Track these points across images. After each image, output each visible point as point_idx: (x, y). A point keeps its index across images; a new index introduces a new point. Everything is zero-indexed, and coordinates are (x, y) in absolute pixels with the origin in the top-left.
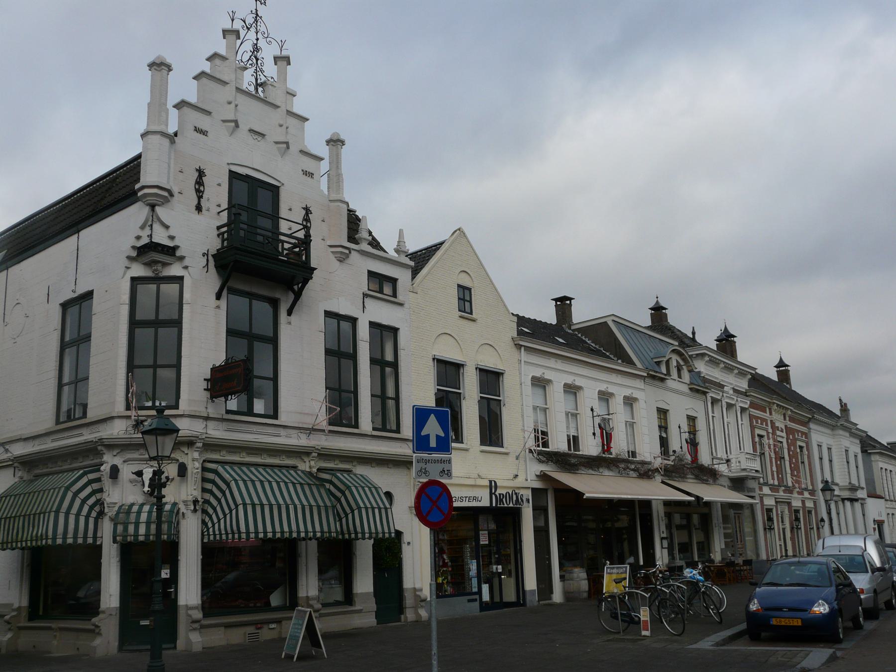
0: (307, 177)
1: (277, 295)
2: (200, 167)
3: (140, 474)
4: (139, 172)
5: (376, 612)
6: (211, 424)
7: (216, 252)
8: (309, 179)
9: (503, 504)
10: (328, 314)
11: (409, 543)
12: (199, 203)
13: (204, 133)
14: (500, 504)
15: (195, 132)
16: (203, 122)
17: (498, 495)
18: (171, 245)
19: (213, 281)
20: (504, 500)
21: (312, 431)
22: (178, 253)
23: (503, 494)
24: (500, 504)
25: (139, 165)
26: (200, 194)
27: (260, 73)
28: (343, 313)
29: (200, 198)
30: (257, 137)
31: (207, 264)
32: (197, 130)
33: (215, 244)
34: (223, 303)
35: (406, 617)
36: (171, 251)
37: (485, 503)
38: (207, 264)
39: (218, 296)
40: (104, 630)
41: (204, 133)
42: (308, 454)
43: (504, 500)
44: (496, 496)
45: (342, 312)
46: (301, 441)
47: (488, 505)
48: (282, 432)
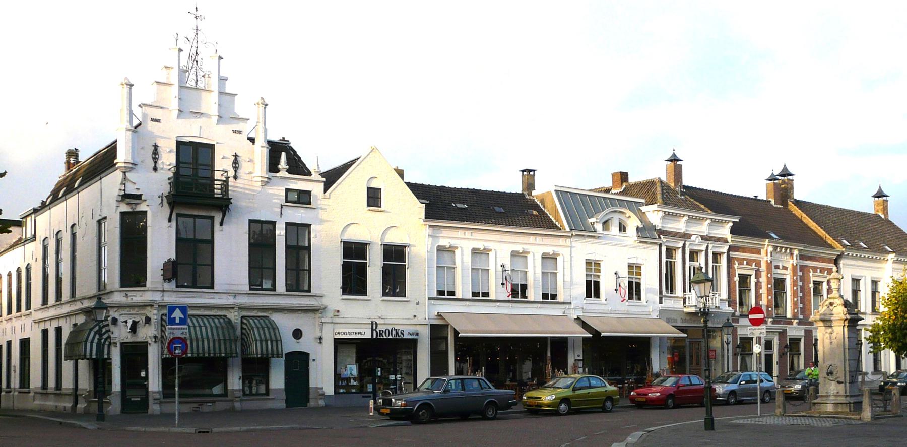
0: (237, 134)
1: (212, 214)
2: (155, 144)
3: (126, 322)
4: (116, 151)
5: (286, 400)
6: (165, 294)
7: (168, 194)
8: (238, 135)
9: (383, 336)
10: (251, 221)
11: (314, 360)
12: (155, 166)
13: (158, 121)
14: (380, 336)
15: (152, 122)
16: (156, 113)
17: (378, 331)
18: (139, 193)
19: (166, 210)
20: (384, 334)
21: (236, 295)
22: (143, 199)
23: (383, 331)
24: (380, 336)
25: (116, 146)
26: (155, 160)
27: (199, 70)
28: (264, 220)
29: (156, 163)
30: (196, 115)
31: (162, 202)
32: (153, 120)
33: (166, 189)
34: (174, 223)
35: (310, 404)
36: (139, 197)
37: (368, 335)
38: (162, 202)
39: (170, 220)
40: (112, 402)
41: (158, 121)
42: (233, 308)
43: (384, 334)
44: (377, 332)
45: (263, 219)
46: (229, 301)
47: (370, 337)
48: (216, 296)
